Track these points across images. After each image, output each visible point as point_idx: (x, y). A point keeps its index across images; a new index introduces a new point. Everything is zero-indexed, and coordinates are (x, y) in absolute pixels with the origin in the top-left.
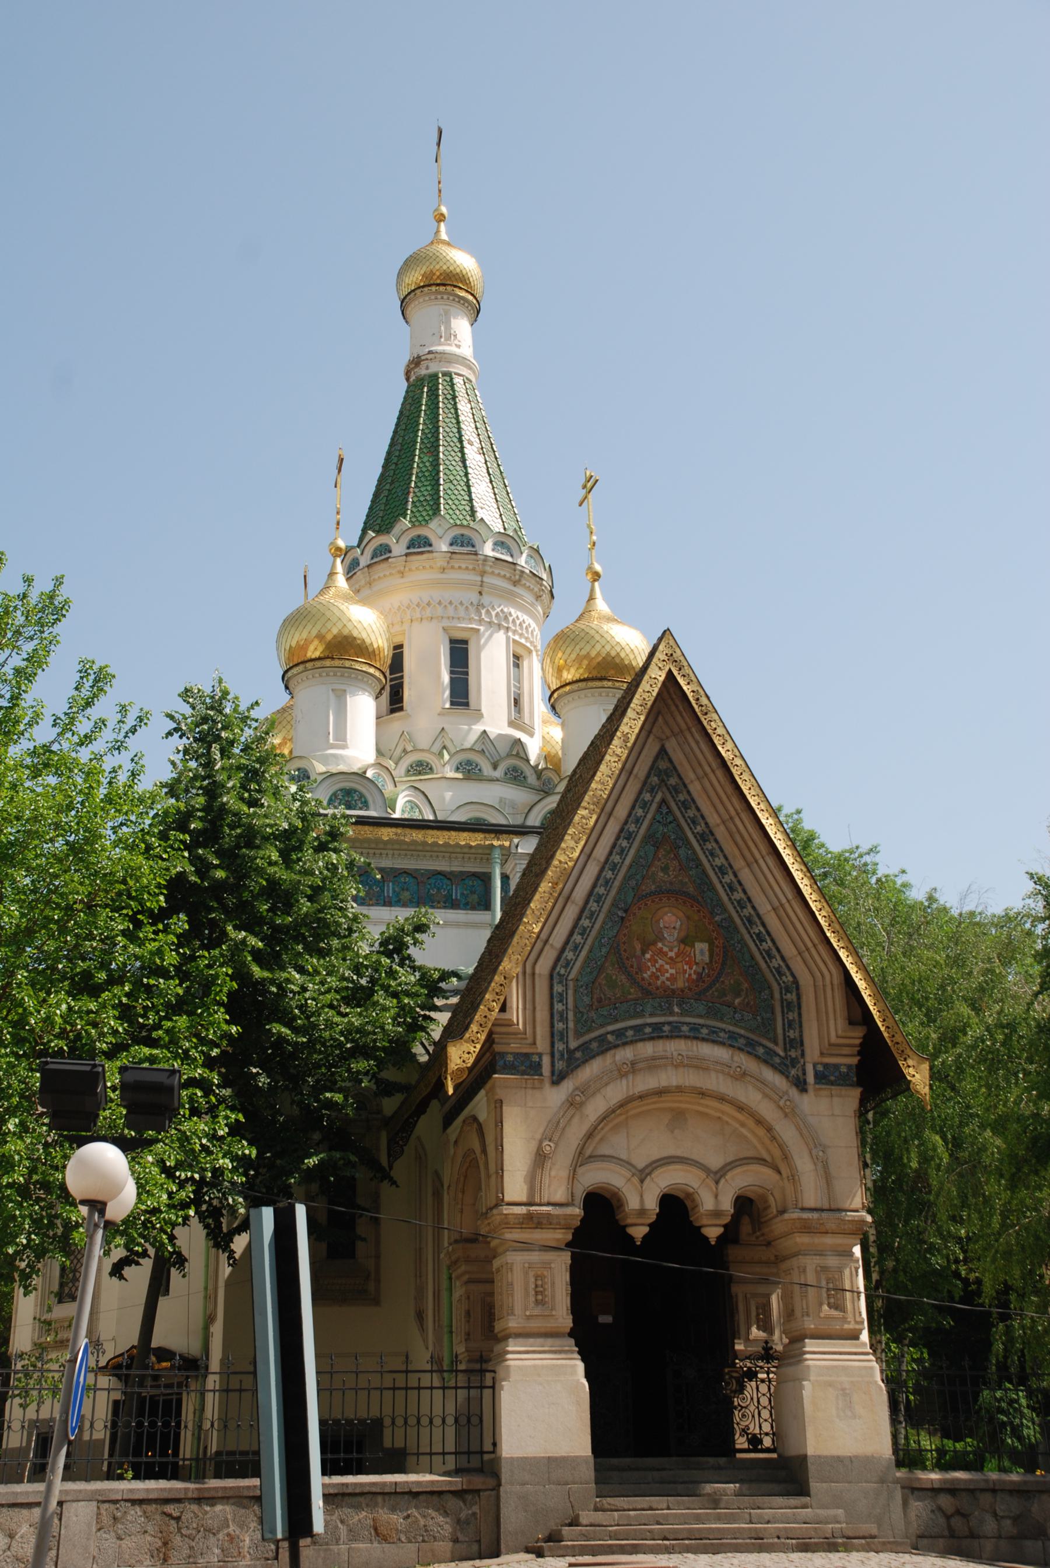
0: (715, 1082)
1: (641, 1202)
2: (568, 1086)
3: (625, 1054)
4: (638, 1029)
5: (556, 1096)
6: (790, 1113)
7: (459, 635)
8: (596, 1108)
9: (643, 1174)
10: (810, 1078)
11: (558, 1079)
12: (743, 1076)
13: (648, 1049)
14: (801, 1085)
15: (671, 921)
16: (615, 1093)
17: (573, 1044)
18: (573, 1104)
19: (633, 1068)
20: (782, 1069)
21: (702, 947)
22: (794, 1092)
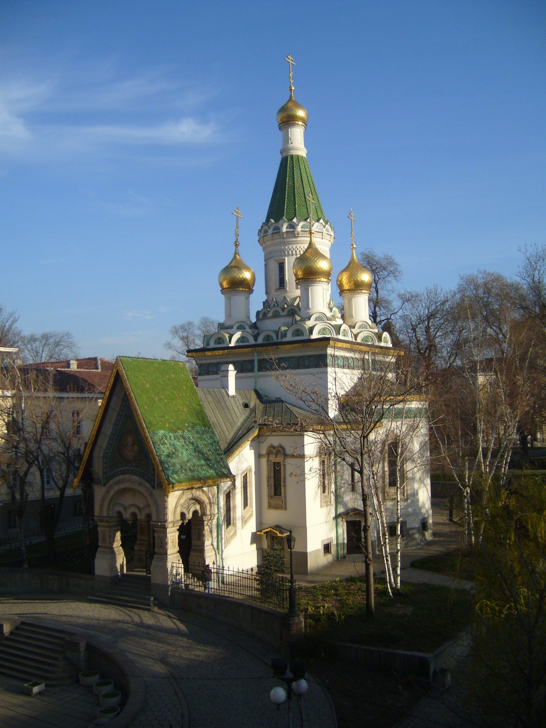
0: (136, 486)
1: (127, 515)
2: (107, 486)
3: (117, 478)
4: (121, 471)
5: (104, 489)
6: (151, 494)
7: (281, 261)
8: (112, 493)
9: (125, 509)
10: (156, 486)
11: (104, 485)
12: (141, 484)
13: (121, 477)
14: (153, 487)
15: (130, 439)
16: (116, 488)
17: (109, 475)
18: (108, 492)
19: (118, 483)
20: (149, 483)
21: (136, 447)
22: (152, 489)
